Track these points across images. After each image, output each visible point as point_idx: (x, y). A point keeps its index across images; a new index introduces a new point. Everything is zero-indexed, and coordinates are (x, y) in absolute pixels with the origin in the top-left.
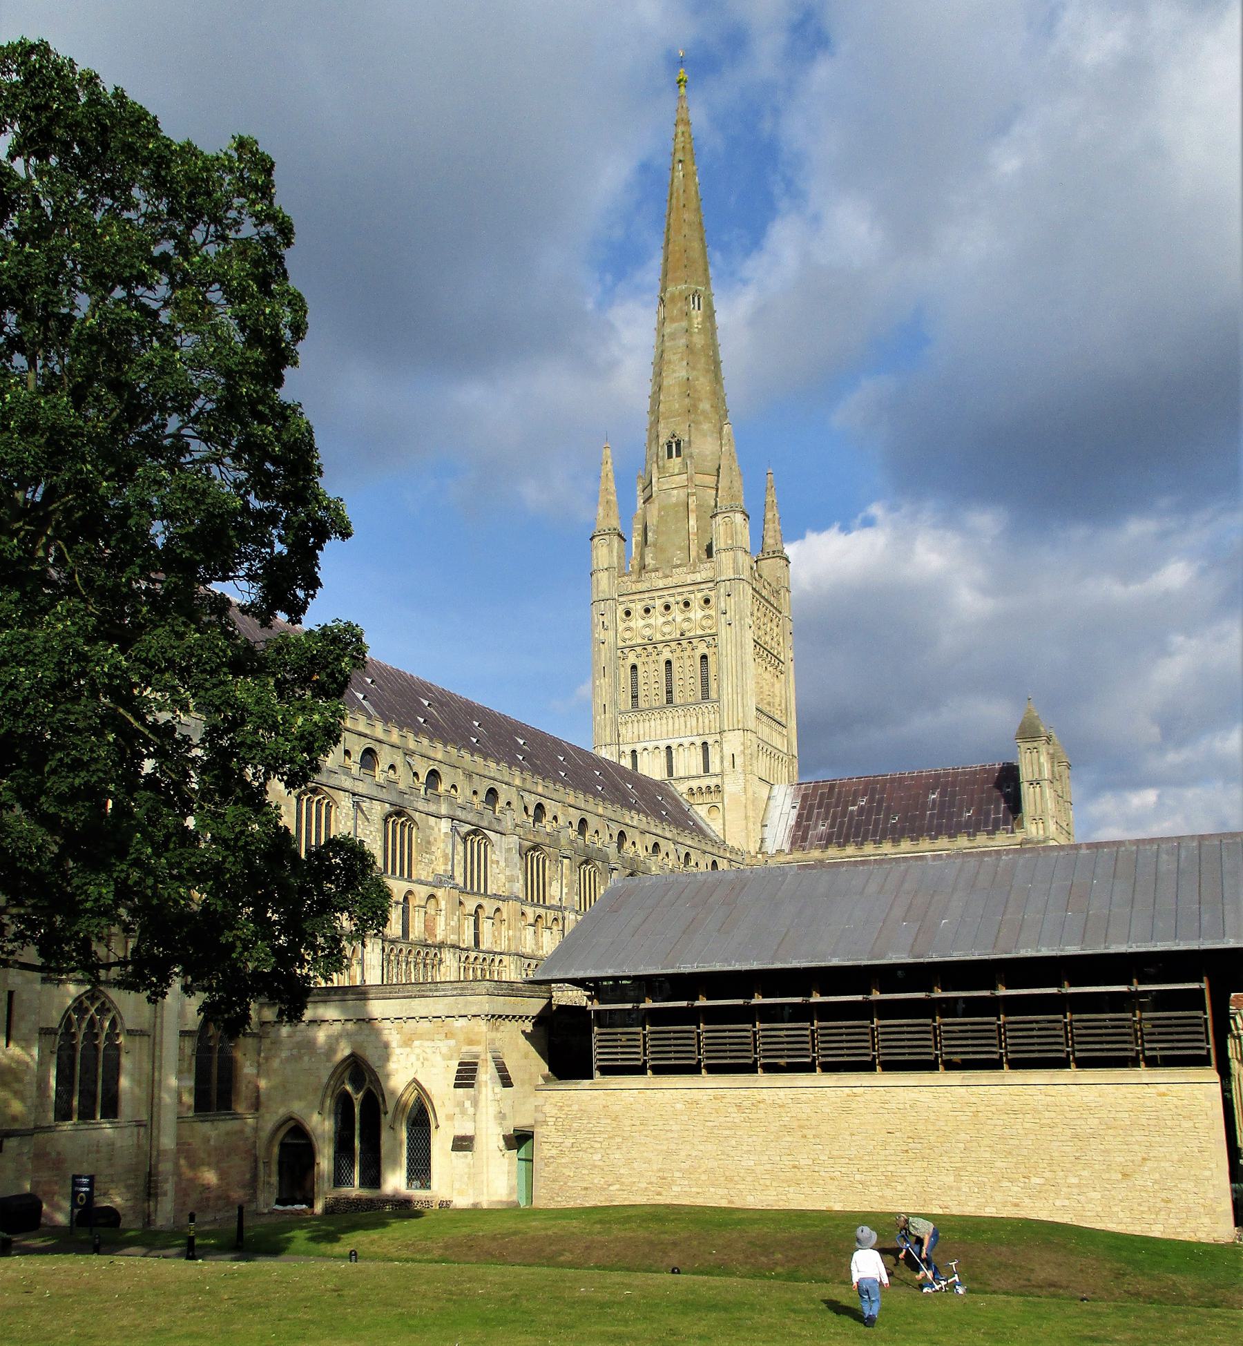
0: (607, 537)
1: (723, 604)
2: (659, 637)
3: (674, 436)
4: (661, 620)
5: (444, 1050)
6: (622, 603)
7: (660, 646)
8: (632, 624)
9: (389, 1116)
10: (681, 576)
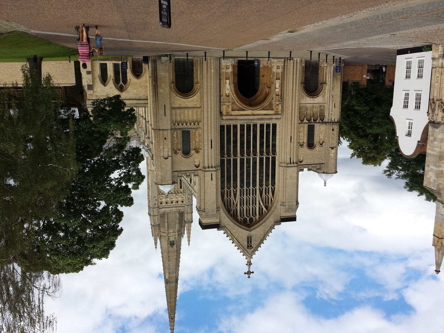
0: (188, 221)
1: (157, 202)
2: (174, 195)
3: (172, 246)
4: (174, 199)
5: (97, 93)
6: (184, 204)
7: (174, 193)
8: (181, 199)
9: (111, 79)
10: (168, 210)
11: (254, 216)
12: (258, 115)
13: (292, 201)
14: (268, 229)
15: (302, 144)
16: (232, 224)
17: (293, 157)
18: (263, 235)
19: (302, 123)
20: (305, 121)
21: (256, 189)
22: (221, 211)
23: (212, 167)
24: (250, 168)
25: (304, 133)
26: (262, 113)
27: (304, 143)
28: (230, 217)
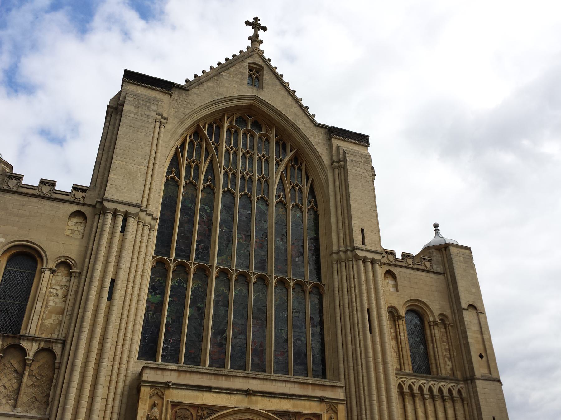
11: (233, 127)
12: (229, 391)
13: (136, 116)
14: (209, 84)
15: (62, 268)
16: (298, 124)
17: (112, 233)
18: (223, 78)
19: (47, 341)
20: (35, 347)
21: (226, 184)
22: (326, 160)
23: (365, 260)
24: (238, 242)
25: (46, 307)
26: (215, 395)
27: (53, 272)
28: (302, 142)
